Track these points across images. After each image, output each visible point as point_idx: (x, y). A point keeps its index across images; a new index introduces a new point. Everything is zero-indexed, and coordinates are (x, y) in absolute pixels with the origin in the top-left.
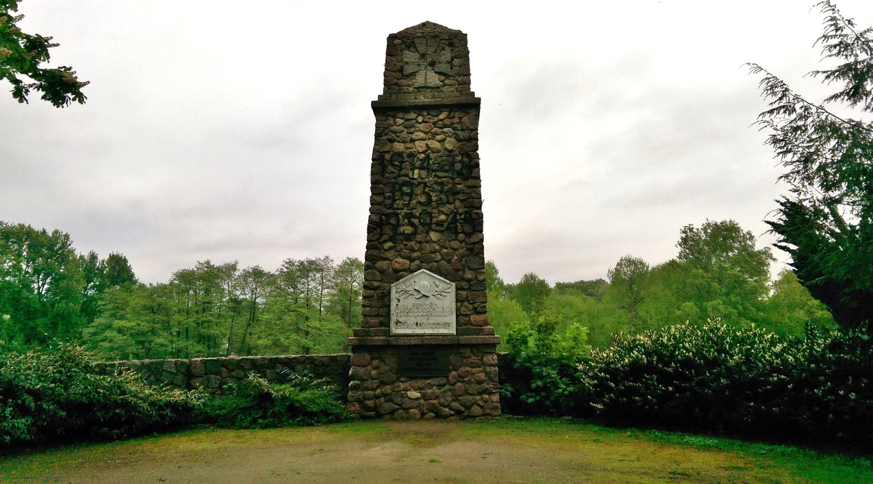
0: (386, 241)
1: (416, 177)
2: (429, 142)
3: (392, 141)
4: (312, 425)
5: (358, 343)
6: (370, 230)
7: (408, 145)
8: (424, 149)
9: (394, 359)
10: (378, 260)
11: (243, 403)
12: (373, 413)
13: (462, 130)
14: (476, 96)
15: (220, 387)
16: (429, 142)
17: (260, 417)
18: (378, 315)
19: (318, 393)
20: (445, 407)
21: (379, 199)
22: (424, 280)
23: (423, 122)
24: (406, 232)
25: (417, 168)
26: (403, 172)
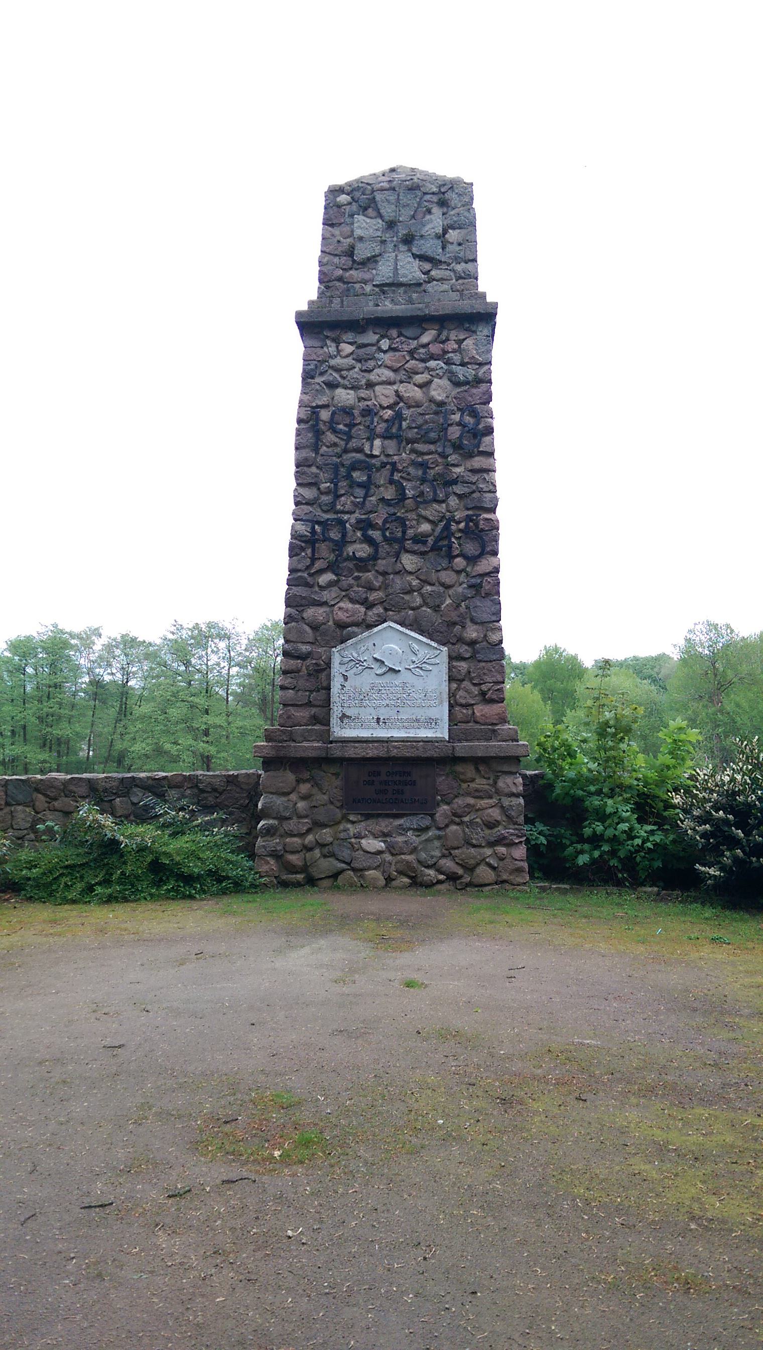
0: (321, 572)
1: (376, 452)
2: (402, 388)
3: (332, 386)
4: (191, 897)
5: (272, 753)
6: (294, 551)
7: (363, 393)
8: (392, 401)
9: (338, 782)
10: (308, 606)
11: (72, 856)
12: (300, 877)
13: (463, 364)
14: (489, 299)
15: (33, 828)
16: (402, 388)
17: (99, 884)
18: (309, 704)
19: (201, 842)
20: (428, 867)
21: (309, 493)
22: (391, 642)
23: (391, 349)
24: (358, 555)
25: (379, 436)
26: (353, 444)
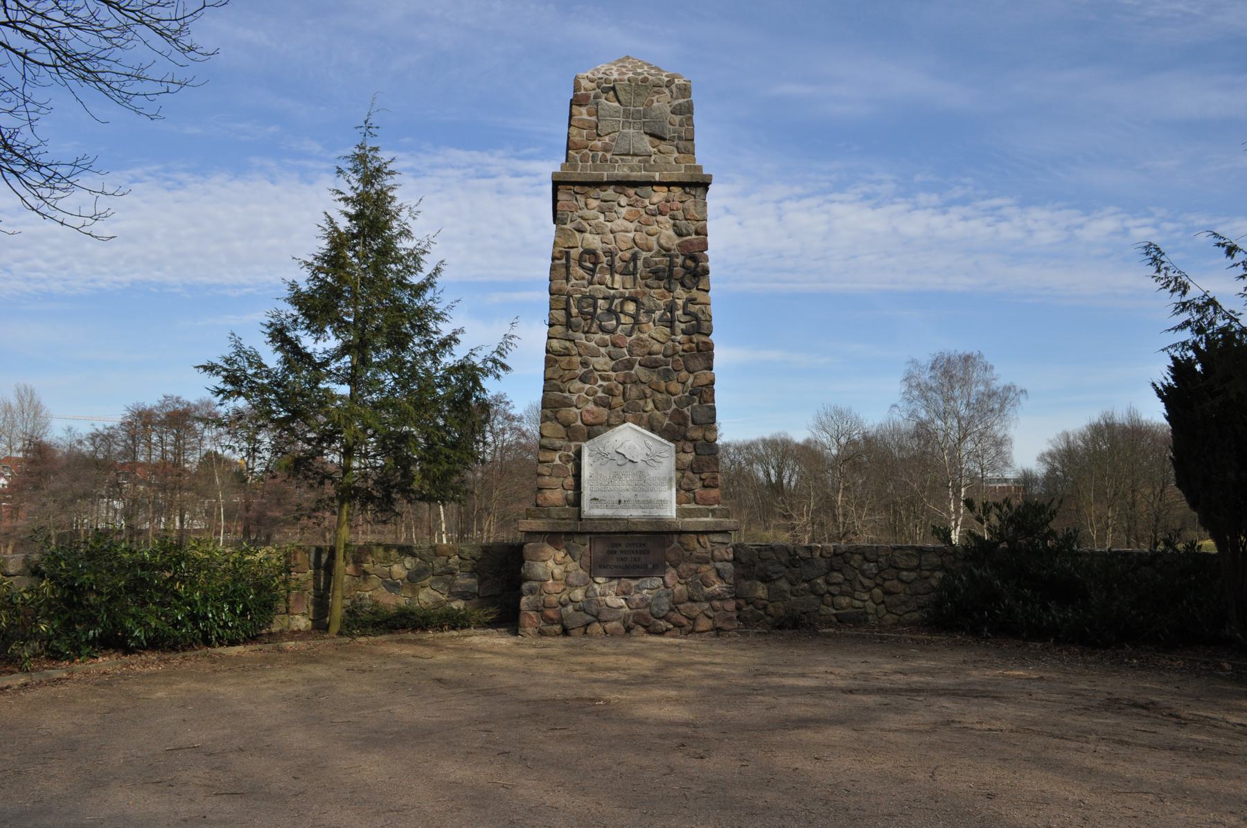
12: (557, 628)
20: (660, 619)
22: (628, 438)
